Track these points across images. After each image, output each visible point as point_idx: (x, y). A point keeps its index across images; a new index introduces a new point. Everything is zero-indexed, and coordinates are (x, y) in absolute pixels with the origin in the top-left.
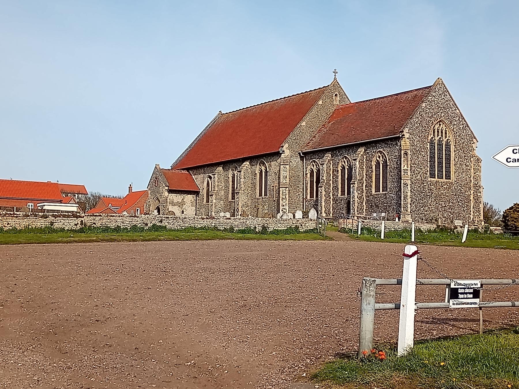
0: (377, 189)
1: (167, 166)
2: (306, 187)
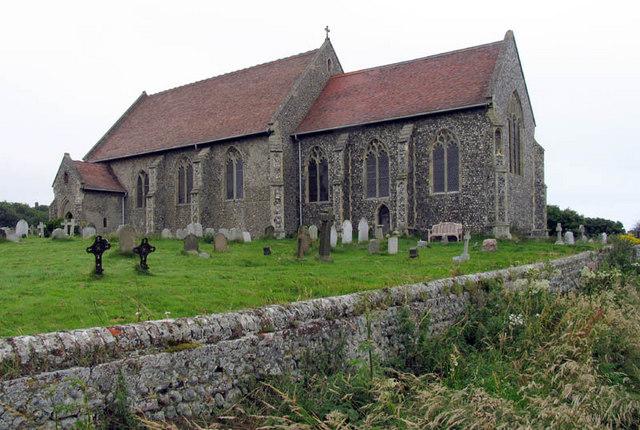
0: (439, 187)
1: (78, 156)
2: (303, 186)
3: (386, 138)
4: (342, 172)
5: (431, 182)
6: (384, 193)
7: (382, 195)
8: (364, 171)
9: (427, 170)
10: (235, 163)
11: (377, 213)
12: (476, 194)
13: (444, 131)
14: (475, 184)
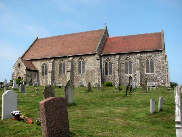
0: (148, 72)
2: (104, 70)
3: (132, 57)
4: (118, 66)
5: (145, 70)
6: (131, 73)
7: (130, 74)
8: (124, 66)
9: (144, 67)
10: (82, 62)
11: (128, 78)
12: (159, 74)
13: (149, 56)
14: (159, 71)
